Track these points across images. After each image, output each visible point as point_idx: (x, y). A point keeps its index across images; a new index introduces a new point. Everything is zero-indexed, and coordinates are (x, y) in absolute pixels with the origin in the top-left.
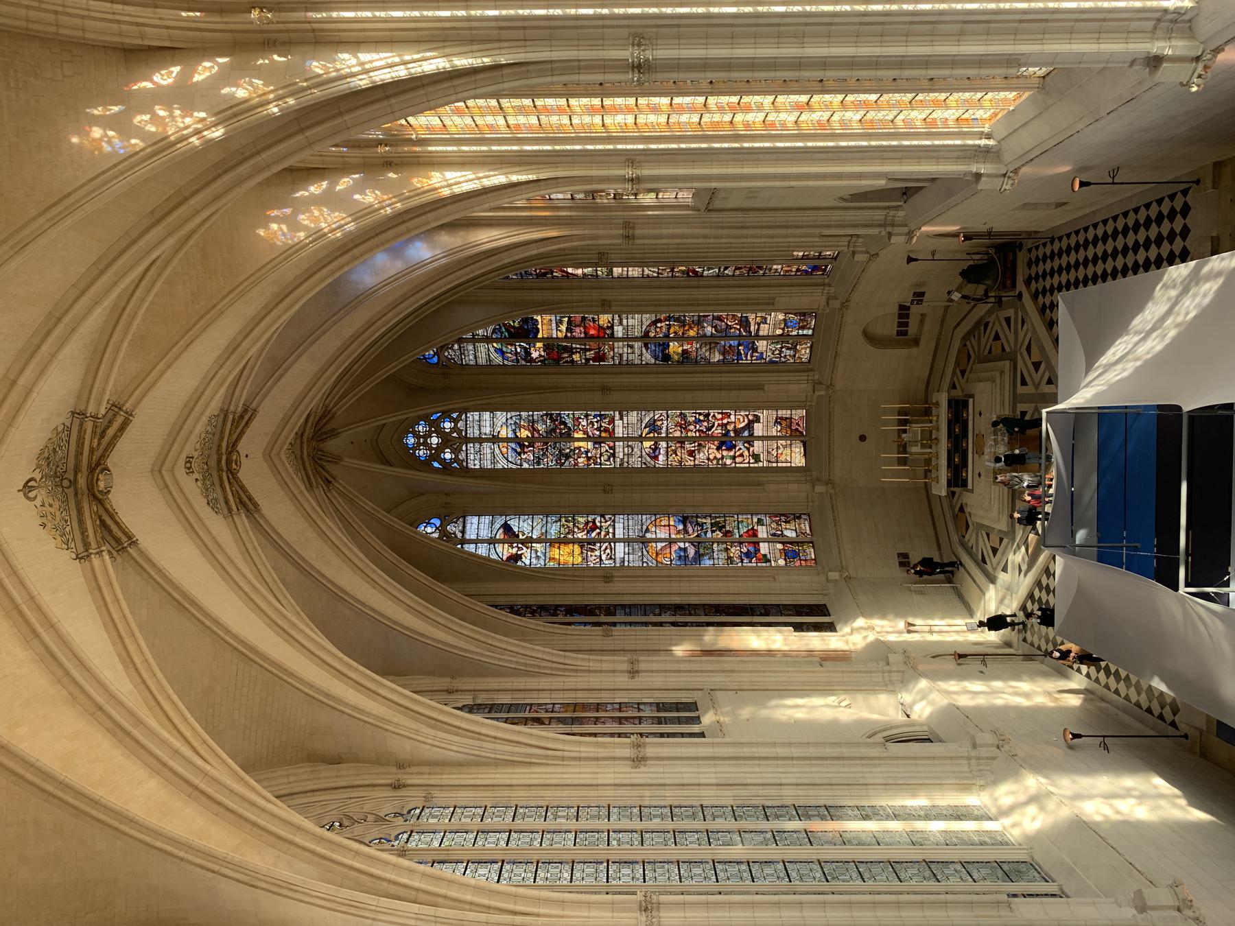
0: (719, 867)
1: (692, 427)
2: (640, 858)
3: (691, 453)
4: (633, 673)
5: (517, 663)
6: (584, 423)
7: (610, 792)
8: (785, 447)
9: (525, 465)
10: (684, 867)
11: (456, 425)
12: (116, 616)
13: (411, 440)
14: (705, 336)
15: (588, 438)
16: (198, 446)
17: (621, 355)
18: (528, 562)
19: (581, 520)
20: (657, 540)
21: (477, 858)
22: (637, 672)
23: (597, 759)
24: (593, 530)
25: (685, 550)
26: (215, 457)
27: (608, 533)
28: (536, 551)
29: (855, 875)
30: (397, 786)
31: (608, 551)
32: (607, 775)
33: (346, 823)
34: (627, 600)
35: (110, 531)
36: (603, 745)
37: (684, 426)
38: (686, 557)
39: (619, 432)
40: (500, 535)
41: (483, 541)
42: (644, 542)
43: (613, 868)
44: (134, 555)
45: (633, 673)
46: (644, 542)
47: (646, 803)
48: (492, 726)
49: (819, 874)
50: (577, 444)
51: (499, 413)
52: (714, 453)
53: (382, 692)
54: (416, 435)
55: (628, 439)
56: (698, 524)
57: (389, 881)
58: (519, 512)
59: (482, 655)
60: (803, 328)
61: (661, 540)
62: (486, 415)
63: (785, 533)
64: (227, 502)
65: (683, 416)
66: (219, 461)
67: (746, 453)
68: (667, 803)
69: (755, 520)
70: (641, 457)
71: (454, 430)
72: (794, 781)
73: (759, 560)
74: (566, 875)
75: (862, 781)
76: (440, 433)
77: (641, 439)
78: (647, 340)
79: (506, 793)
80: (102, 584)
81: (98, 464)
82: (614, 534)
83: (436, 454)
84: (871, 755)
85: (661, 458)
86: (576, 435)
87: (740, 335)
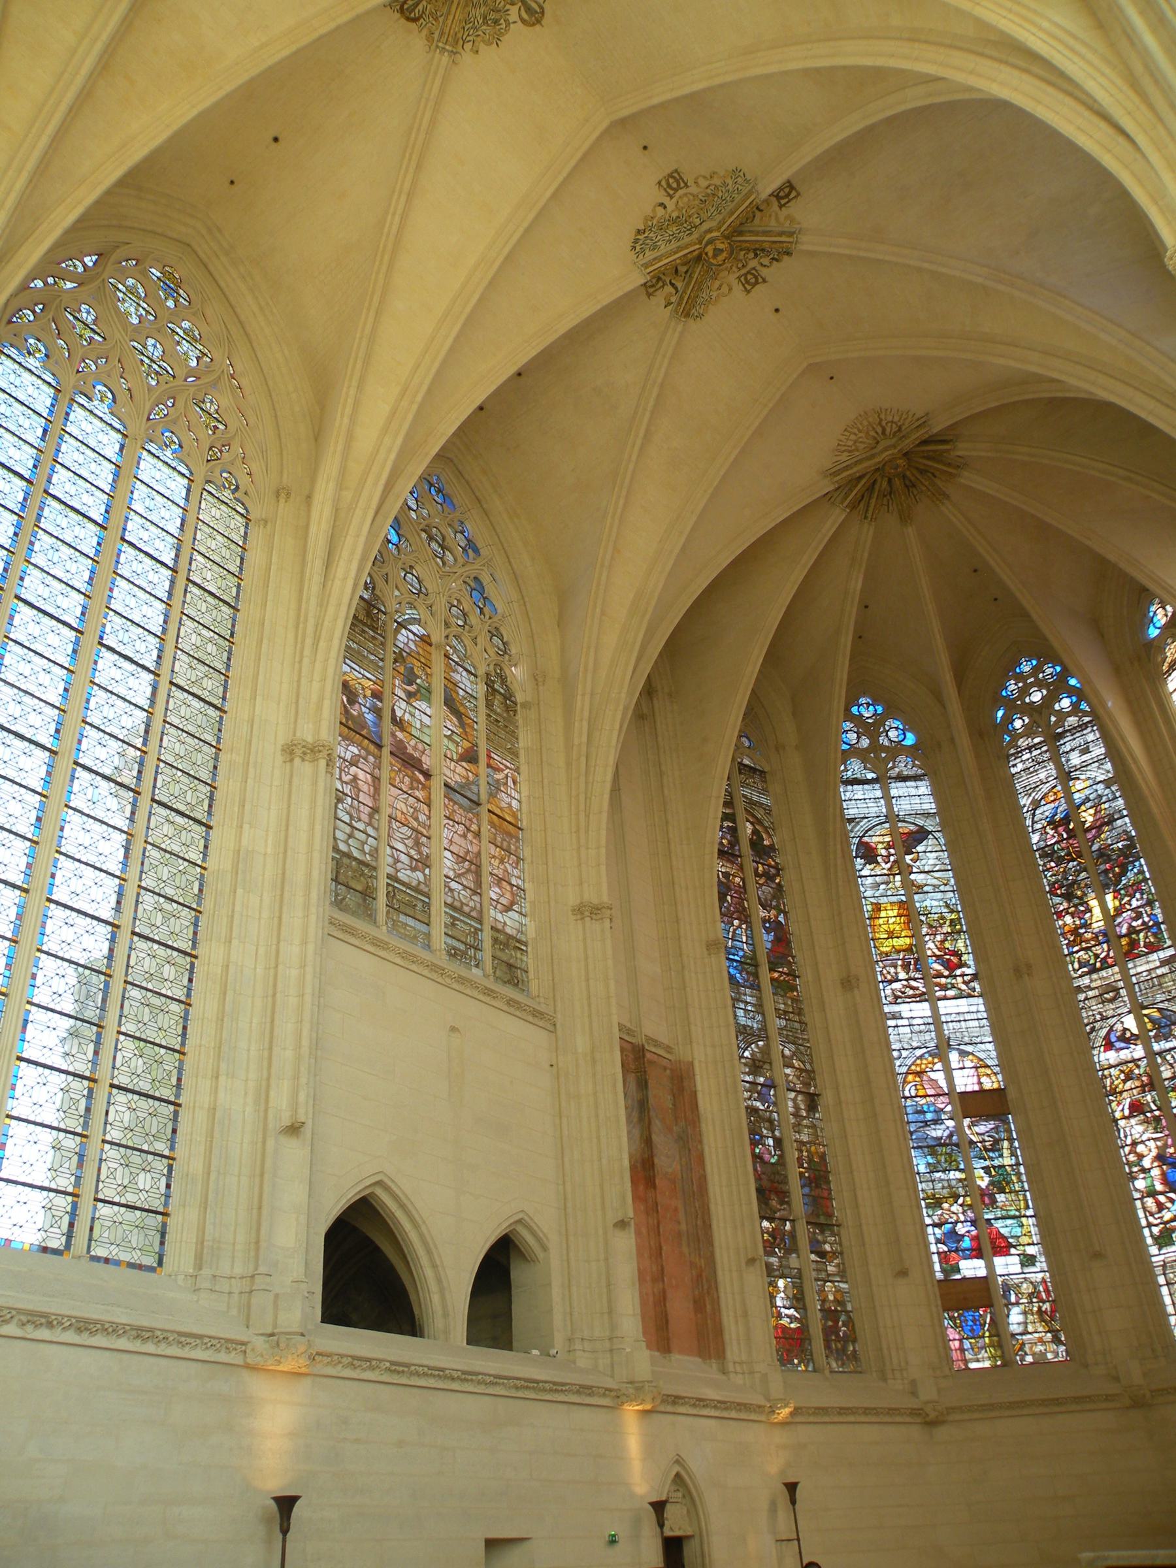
3: (1137, 1108)
6: (1135, 903)
9: (1035, 838)
11: (1069, 714)
13: (1026, 668)
15: (1110, 919)
16: (703, 183)
18: (863, 873)
19: (960, 944)
20: (948, 1071)
25: (937, 1121)
26: (714, 224)
27: (944, 988)
28: (887, 883)
31: (911, 992)
34: (812, 1016)
38: (926, 1123)
39: (1140, 967)
40: (904, 828)
41: (889, 806)
42: (942, 1049)
46: (942, 1049)
50: (1094, 903)
51: (1109, 766)
52: (1149, 1151)
54: (1036, 670)
55: (1130, 987)
56: (996, 1142)
58: (952, 847)
62: (1098, 751)
66: (710, 231)
69: (1031, 1250)
70: (1104, 1018)
71: (1062, 715)
76: (1049, 701)
77: (1137, 1009)
82: (945, 998)
83: (1014, 707)
85: (1111, 1057)
86: (1109, 897)
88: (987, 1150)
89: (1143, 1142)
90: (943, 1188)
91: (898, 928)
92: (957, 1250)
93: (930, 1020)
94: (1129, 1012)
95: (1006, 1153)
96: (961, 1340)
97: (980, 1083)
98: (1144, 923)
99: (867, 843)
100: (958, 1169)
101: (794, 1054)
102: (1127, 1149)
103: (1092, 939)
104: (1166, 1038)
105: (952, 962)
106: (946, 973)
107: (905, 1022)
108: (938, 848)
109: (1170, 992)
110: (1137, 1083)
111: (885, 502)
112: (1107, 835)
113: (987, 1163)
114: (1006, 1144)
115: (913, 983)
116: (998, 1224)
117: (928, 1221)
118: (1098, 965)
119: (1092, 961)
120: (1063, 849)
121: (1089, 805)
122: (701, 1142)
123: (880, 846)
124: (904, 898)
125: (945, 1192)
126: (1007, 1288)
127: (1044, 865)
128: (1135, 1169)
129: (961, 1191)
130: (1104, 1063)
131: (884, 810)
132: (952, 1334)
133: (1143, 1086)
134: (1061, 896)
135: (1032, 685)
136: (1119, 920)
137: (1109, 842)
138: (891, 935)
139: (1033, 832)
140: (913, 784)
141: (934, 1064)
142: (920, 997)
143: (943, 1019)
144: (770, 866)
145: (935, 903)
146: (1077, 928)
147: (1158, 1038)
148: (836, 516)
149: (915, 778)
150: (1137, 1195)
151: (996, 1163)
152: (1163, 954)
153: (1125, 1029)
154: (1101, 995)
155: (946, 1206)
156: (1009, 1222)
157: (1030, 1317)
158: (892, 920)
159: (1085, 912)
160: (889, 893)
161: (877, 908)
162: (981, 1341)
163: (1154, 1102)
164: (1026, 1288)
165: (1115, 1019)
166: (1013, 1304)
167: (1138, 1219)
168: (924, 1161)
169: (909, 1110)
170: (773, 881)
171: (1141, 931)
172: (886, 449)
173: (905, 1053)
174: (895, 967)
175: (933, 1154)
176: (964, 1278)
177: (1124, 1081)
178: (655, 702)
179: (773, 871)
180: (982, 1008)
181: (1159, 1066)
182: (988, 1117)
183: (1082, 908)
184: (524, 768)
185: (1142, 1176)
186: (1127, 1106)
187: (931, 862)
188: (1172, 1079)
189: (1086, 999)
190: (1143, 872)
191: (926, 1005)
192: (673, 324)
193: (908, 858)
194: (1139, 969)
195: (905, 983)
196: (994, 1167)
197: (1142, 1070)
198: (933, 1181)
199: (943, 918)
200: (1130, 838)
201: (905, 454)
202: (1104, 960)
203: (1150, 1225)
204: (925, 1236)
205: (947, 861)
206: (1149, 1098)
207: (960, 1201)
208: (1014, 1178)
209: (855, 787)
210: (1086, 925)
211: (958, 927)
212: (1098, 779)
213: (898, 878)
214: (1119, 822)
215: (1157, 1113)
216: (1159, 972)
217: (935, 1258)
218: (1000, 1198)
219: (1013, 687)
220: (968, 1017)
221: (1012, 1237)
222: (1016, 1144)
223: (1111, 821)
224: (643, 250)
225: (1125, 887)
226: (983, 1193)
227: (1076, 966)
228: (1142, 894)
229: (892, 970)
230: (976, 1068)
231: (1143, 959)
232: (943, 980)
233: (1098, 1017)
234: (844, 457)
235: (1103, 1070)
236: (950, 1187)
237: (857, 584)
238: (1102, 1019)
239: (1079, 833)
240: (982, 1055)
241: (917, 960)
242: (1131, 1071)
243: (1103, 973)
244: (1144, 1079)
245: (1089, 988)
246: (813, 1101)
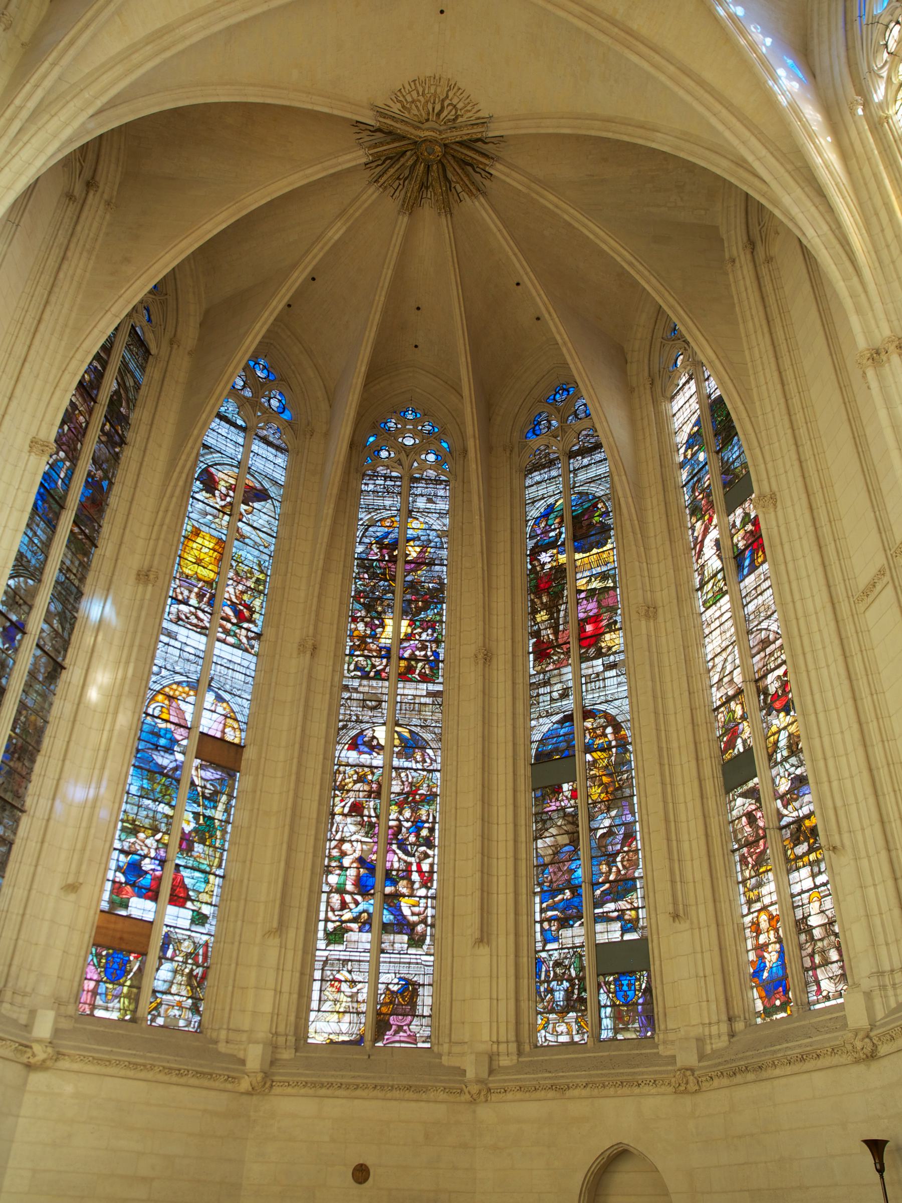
1: (407, 813)
3: (357, 809)
6: (424, 636)
8: (353, 997)
14: (591, 818)
17: (546, 683)
20: (199, 708)
24: (238, 614)
25: (169, 750)
27: (227, 632)
28: (215, 517)
31: (195, 621)
37: (411, 798)
38: (156, 747)
40: (251, 481)
51: (447, 521)
52: (353, 851)
56: (216, 793)
58: (286, 519)
60: (617, 1017)
61: (197, 716)
62: (443, 506)
63: (167, 966)
65: (430, 798)
67: (347, 915)
70: (359, 721)
71: (424, 464)
73: (117, 888)
78: (577, 717)
82: (224, 641)
85: (352, 756)
87: (595, 885)
88: (204, 797)
89: (351, 841)
90: (147, 817)
91: (207, 559)
93: (202, 655)
94: (384, 724)
95: (221, 807)
96: (98, 982)
97: (223, 732)
98: (426, 655)
99: (212, 474)
100: (168, 804)
101: (59, 614)
102: (334, 843)
103: (375, 651)
104: (408, 757)
105: (243, 615)
106: (234, 621)
107: (178, 645)
108: (273, 514)
109: (426, 720)
110: (366, 788)
111: (395, 186)
112: (422, 573)
113: (200, 810)
114: (224, 798)
115: (200, 614)
116: (185, 873)
118: (372, 674)
119: (367, 669)
120: (380, 568)
121: (417, 543)
123: (222, 483)
124: (224, 537)
125: (147, 823)
126: (167, 940)
127: (358, 573)
128: (334, 864)
129: (163, 828)
130: (344, 760)
133: (370, 792)
134: (363, 604)
135: (409, 431)
136: (405, 644)
137: (423, 579)
138: (199, 562)
139: (360, 543)
140: (274, 451)
141: (188, 695)
142: (203, 630)
144: (117, 431)
145: (251, 558)
146: (365, 636)
147: (399, 755)
148: (357, 157)
149: (278, 448)
150: (326, 888)
151: (208, 813)
152: (431, 687)
153: (374, 737)
154: (364, 700)
155: (142, 835)
156: (197, 874)
157: (179, 978)
158: (205, 550)
159: (378, 626)
160: (213, 526)
161: (197, 532)
162: (118, 988)
163: (375, 809)
164: (187, 947)
165: (368, 725)
166: (167, 959)
167: (318, 911)
168: (139, 783)
170: (114, 447)
171: (421, 660)
172: (433, 130)
174: (190, 592)
175: (151, 780)
176: (129, 917)
177: (355, 782)
178: (91, 194)
179: (117, 438)
180: (253, 666)
181: (391, 779)
182: (217, 766)
183: (377, 622)
185: (338, 872)
186: (349, 805)
187: (261, 521)
188: (399, 794)
189: (349, 698)
190: (442, 615)
191: (204, 639)
194: (406, 692)
195: (193, 610)
196: (204, 816)
197: (375, 778)
198: (139, 806)
199: (251, 573)
200: (442, 584)
201: (445, 145)
202: (378, 673)
203: (327, 920)
205: (275, 529)
206: (372, 804)
207: (158, 836)
208: (218, 833)
209: (223, 423)
210: (374, 637)
211: (261, 588)
212: (434, 527)
213: (226, 518)
214: (437, 568)
215: (374, 820)
216: (423, 700)
218: (198, 848)
219: (392, 425)
220: (237, 668)
221: (194, 890)
222: (233, 802)
223: (432, 563)
225: (422, 621)
227: (352, 667)
228: (434, 632)
229: (186, 593)
230: (226, 717)
231: (414, 685)
232: (229, 626)
233: (354, 718)
234: (396, 108)
235: (340, 765)
236: (154, 818)
237: (336, 233)
238: (356, 721)
239: (400, 563)
240: (236, 708)
241: (213, 596)
242: (365, 775)
243: (374, 683)
244: (374, 786)
245: (356, 690)
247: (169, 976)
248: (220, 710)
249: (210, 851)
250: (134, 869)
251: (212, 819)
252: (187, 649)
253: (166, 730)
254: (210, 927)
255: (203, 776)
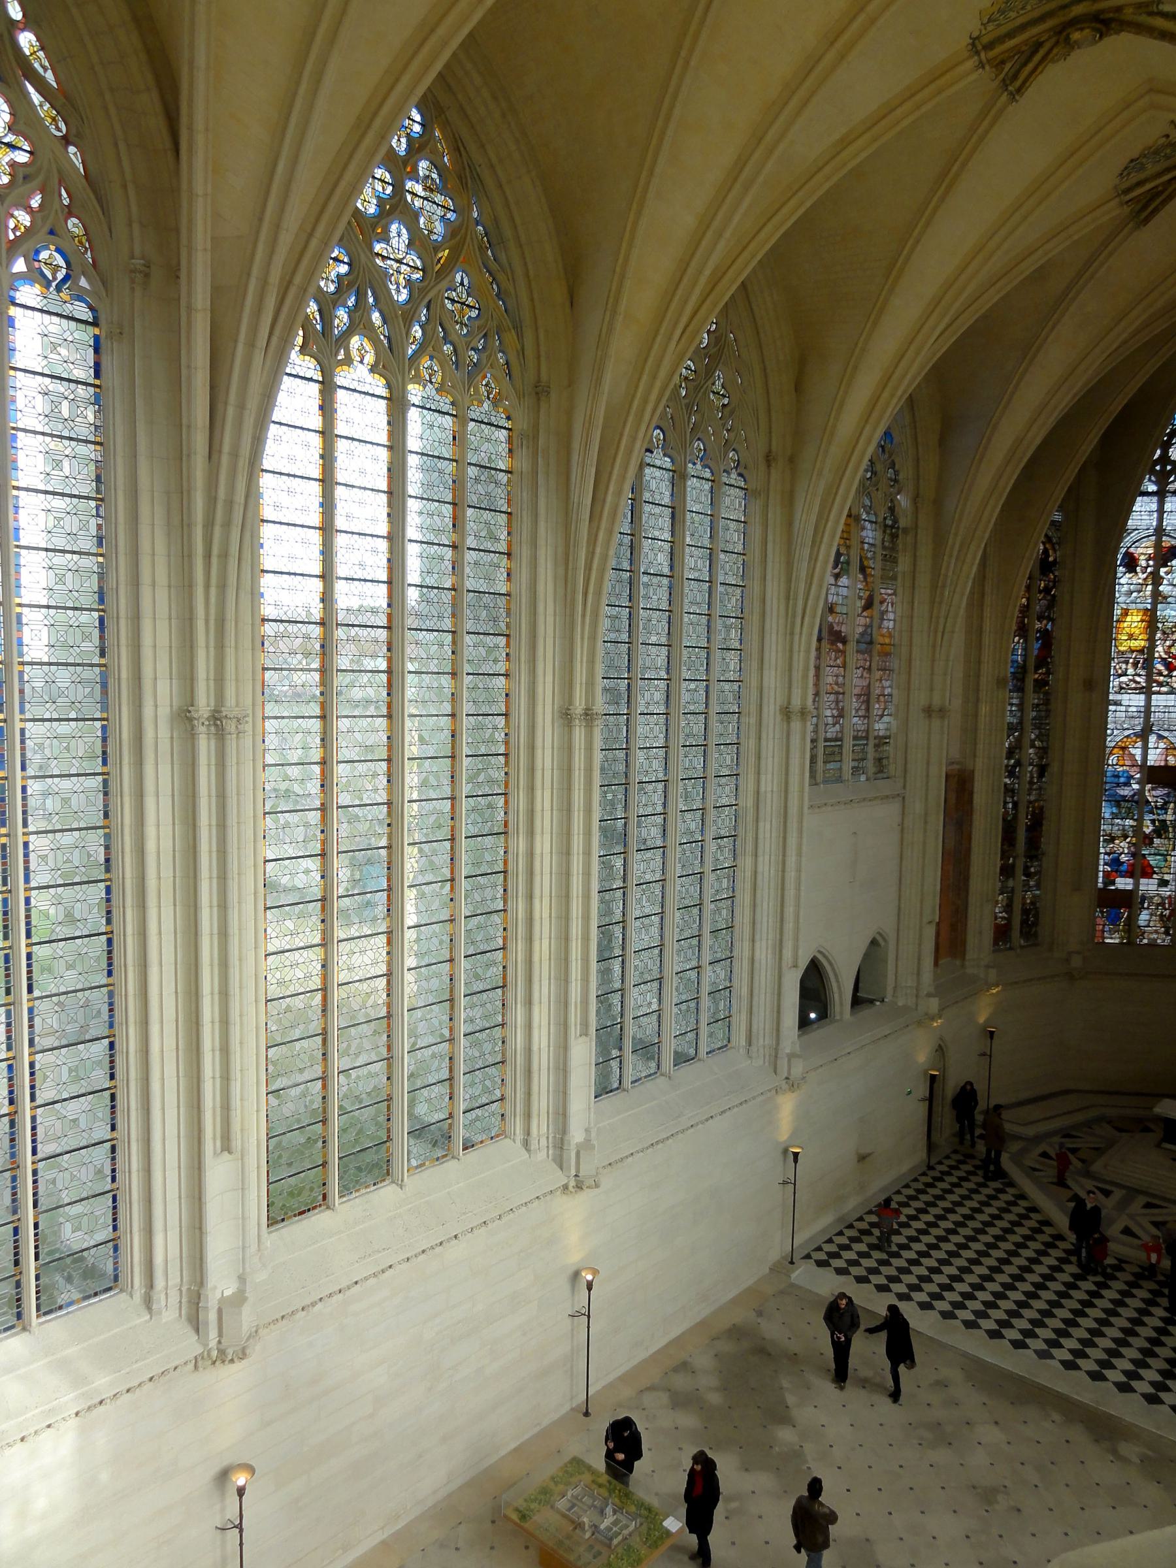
0: (661, 786)
2: (672, 711)
4: (928, 711)
5: (946, 576)
7: (754, 683)
10: (662, 752)
12: (899, 111)
18: (1122, 581)
21: (676, 551)
22: (930, 716)
23: (790, 670)
28: (1139, 592)
29: (647, 911)
30: (769, 459)
32: (772, 679)
33: (727, 410)
35: (1025, 64)
36: (805, 677)
38: (1118, 785)
41: (1160, 520)
43: (662, 684)
44: (999, 104)
45: (928, 711)
47: (742, 720)
48: (829, 556)
49: (648, 877)
53: (868, 428)
56: (1166, 803)
57: (611, 473)
59: (956, 534)
63: (1145, 912)
64: (1140, 184)
68: (742, 741)
69: (1166, 877)
72: (760, 869)
74: (653, 639)
75: (757, 937)
79: (758, 574)
80: (942, 81)
81: (1106, 23)
82: (1159, 693)
84: (784, 951)
88: (1157, 808)
92: (1116, 871)
97: (1166, 761)
101: (1037, 737)
106: (1166, 673)
113: (1155, 817)
115: (1138, 679)
117: (1102, 850)
122: (971, 825)
123: (1142, 557)
124: (1149, 607)
126: (1144, 898)
131: (1155, 523)
132: (1099, 921)
138: (1131, 637)
142: (1140, 690)
143: (1153, 709)
151: (1161, 817)
161: (1126, 613)
164: (1156, 900)
169: (1108, 774)
173: (1116, 732)
174: (1127, 663)
175: (1118, 805)
176: (1117, 889)
184: (900, 591)
191: (1142, 697)
192: (1130, 225)
193: (1163, 571)
204: (1098, 859)
217: (1101, 874)
224: (1129, 174)
226: (1146, 836)
229: (1124, 666)
232: (1162, 678)
236: (1124, 830)
241: (1145, 660)
246: (1042, 770)
247: (1147, 917)
248: (1162, 745)
249: (1166, 842)
250: (1116, 862)
251: (1165, 821)
252: (1131, 709)
253: (1123, 771)
254: (1171, 887)
255: (1154, 795)
